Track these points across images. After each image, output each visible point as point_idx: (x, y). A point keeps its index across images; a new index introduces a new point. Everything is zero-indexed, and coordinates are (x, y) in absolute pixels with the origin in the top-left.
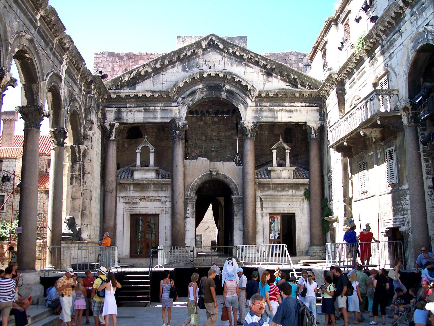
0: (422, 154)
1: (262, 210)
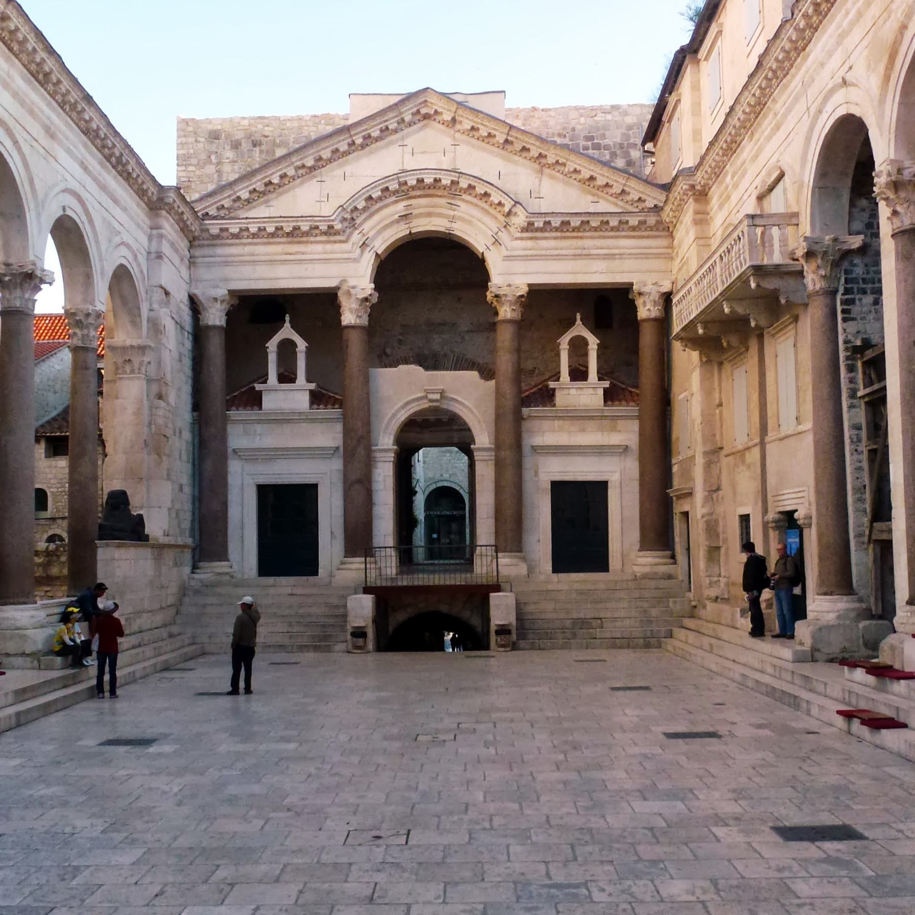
0: (842, 355)
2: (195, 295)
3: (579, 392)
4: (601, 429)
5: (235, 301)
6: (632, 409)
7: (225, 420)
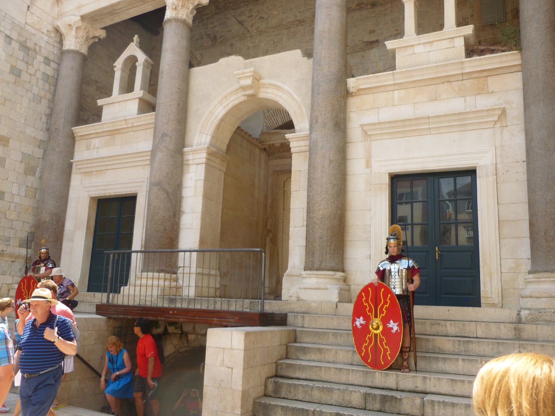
1: (368, 165)
2: (58, 27)
3: (428, 48)
4: (462, 93)
5: (102, 34)
6: (509, 58)
7: (72, 138)
